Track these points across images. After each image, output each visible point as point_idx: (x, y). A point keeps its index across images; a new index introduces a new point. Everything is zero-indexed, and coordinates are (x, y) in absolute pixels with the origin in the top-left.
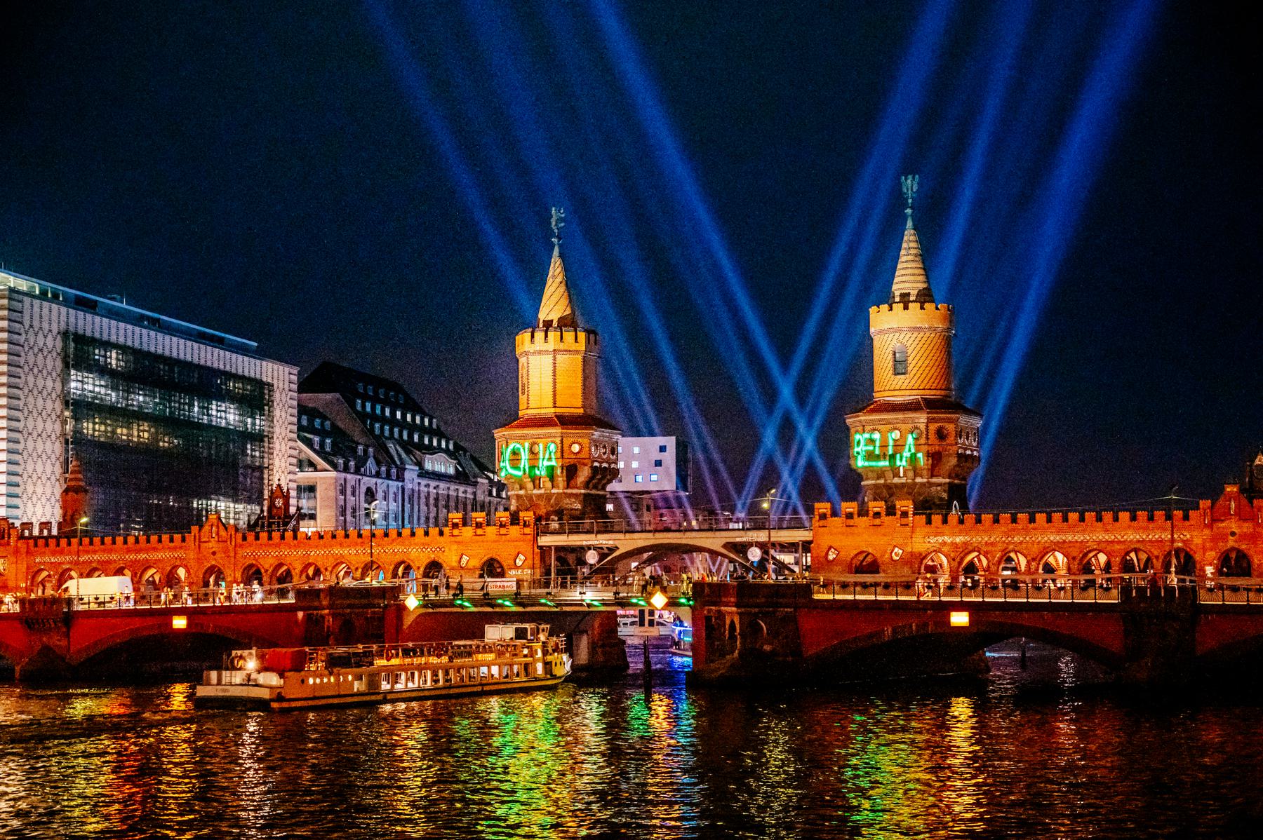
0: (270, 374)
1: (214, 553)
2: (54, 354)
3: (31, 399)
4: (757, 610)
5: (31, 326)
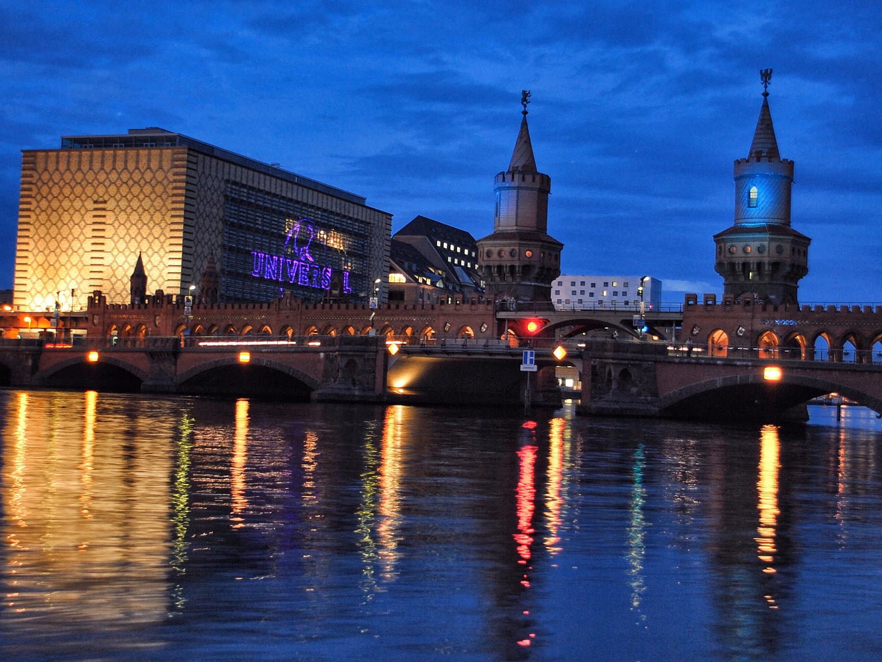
1: (288, 317)
2: (219, 192)
3: (201, 220)
4: (627, 362)
5: (203, 173)
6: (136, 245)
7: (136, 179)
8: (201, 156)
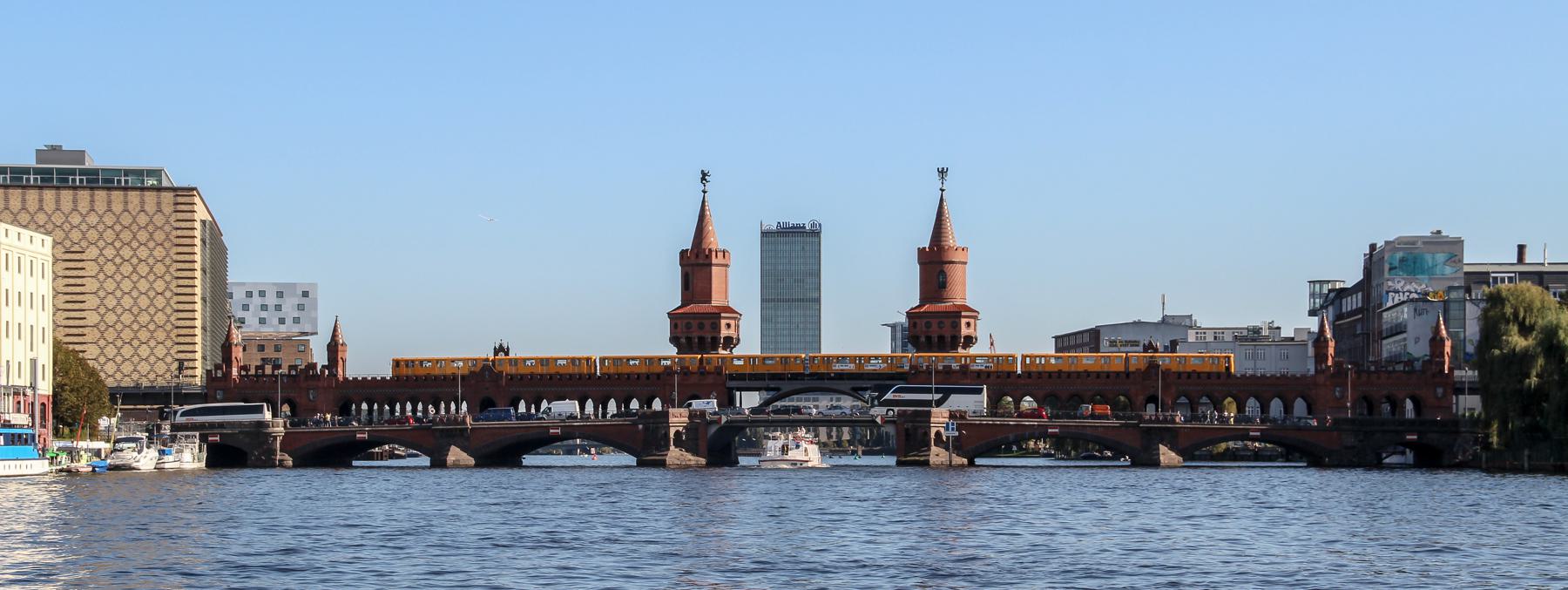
1: (487, 389)
6: (132, 301)
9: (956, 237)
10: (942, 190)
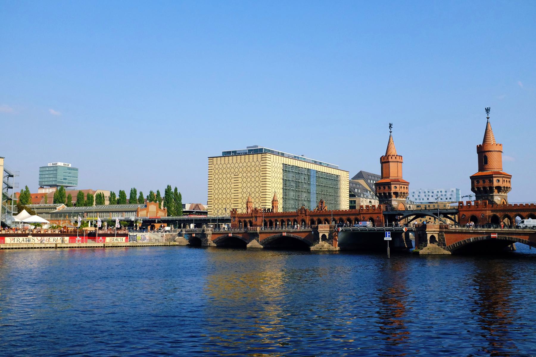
0: (341, 173)
1: (303, 216)
3: (273, 179)
4: (433, 232)
5: (273, 161)
7: (249, 166)
8: (272, 155)
9: (495, 139)
10: (488, 118)
